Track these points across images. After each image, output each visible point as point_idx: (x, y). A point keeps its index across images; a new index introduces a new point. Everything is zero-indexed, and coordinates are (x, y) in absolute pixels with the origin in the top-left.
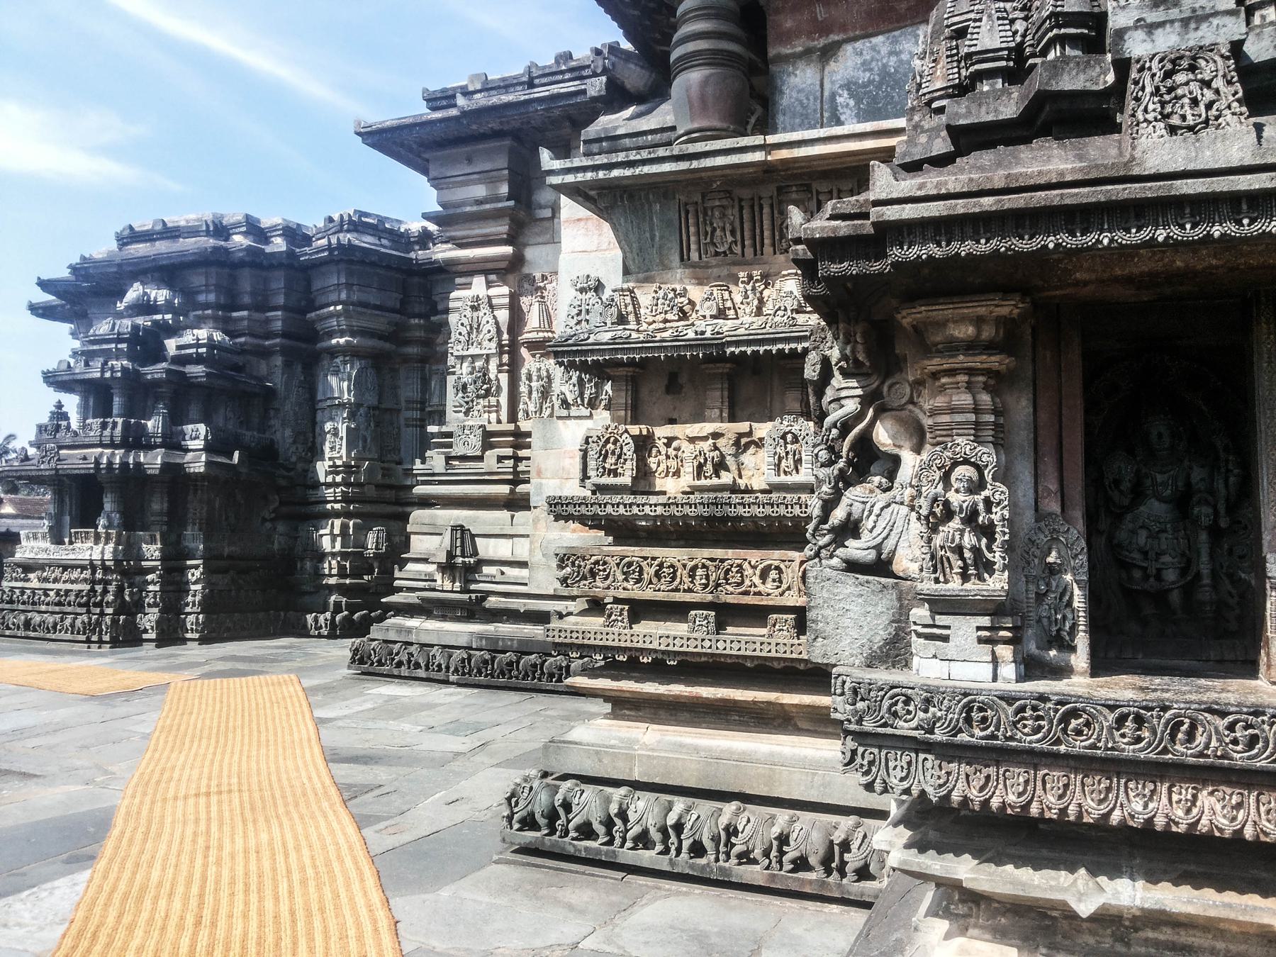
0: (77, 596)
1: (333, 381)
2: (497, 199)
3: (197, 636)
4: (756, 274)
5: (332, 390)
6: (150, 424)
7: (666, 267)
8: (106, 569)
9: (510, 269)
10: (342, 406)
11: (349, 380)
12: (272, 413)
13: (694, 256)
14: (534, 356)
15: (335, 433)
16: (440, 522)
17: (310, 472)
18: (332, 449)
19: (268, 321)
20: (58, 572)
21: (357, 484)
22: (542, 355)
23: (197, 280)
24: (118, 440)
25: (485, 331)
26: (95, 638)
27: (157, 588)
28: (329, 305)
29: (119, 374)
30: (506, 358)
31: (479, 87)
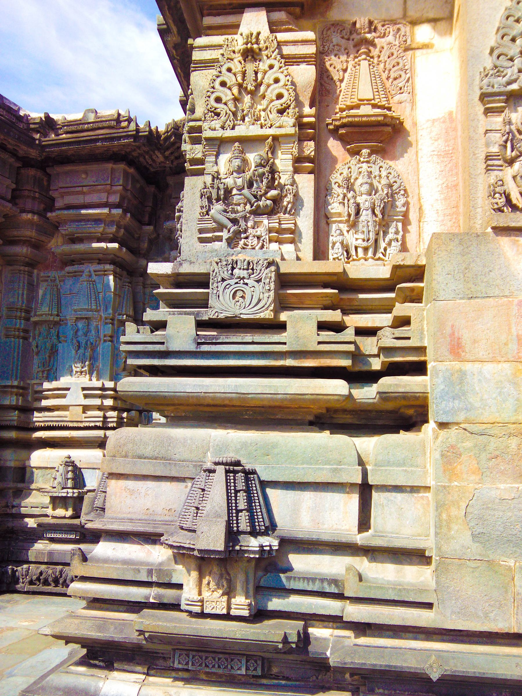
16: (181, 453)
25: (271, 93)
30: (309, 148)
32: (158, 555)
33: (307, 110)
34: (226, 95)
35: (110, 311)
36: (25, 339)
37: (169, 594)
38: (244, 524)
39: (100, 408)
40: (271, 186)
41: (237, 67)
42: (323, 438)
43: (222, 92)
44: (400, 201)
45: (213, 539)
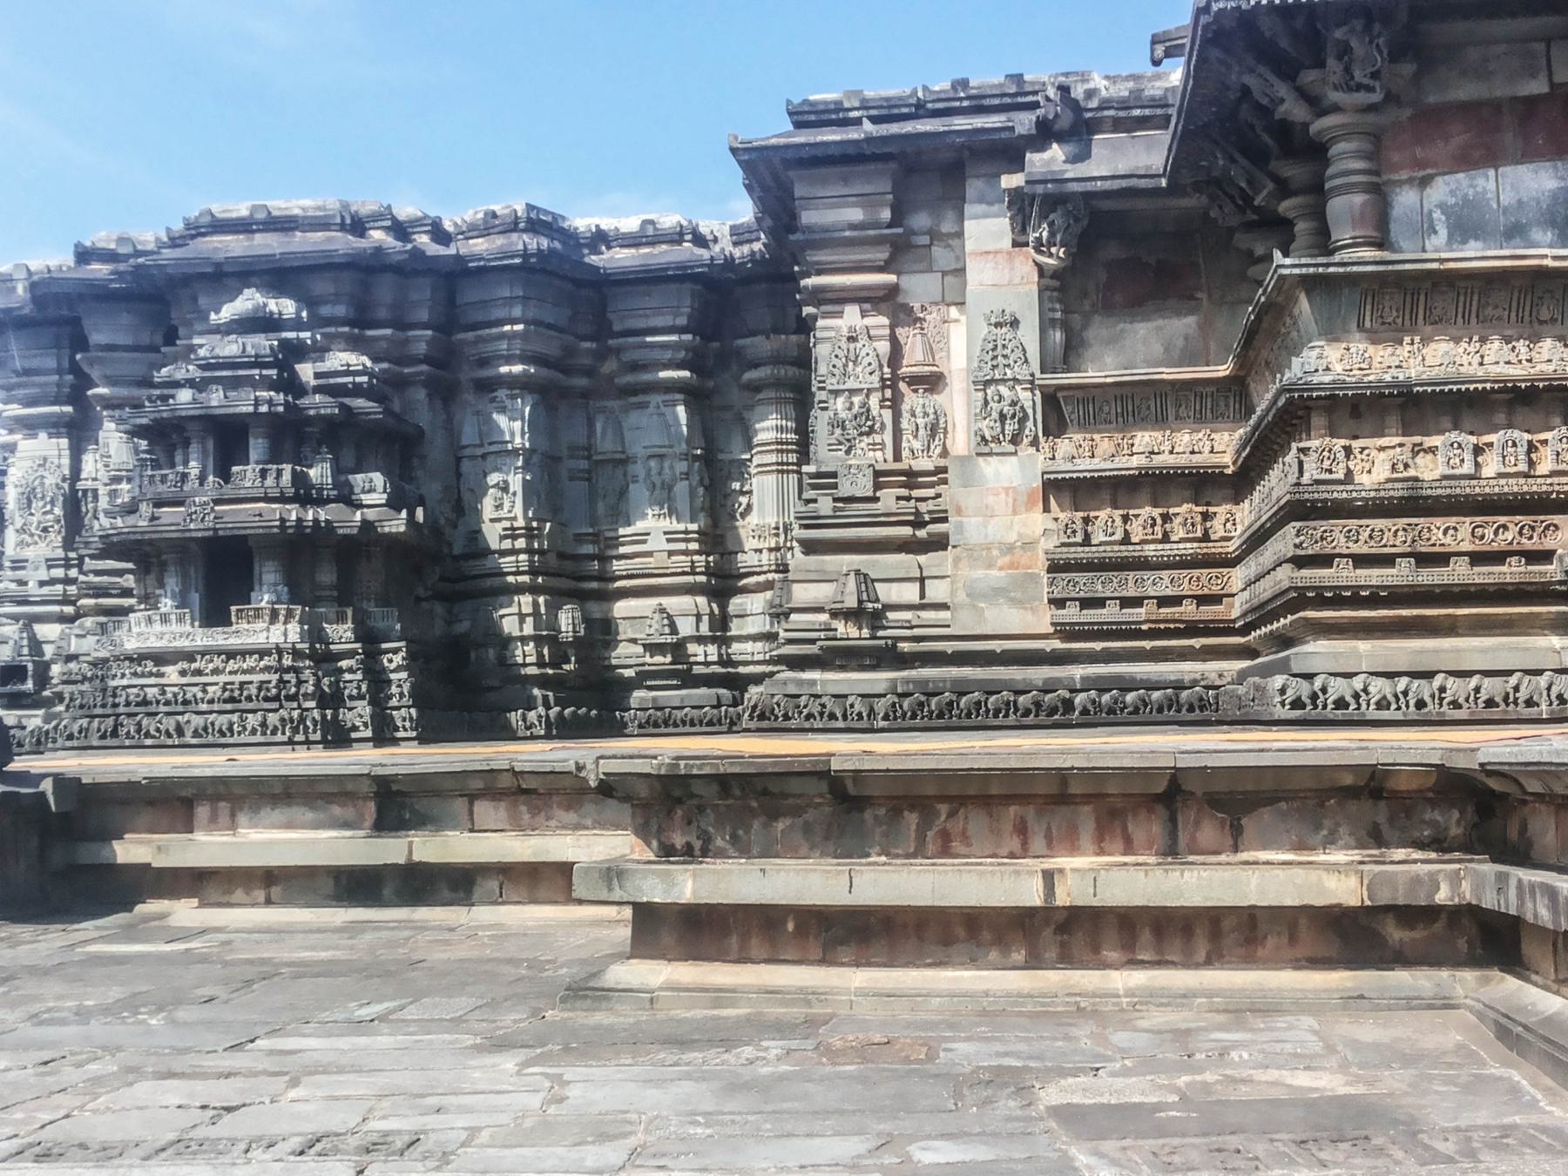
0: (260, 689)
1: (502, 420)
2: (876, 225)
3: (414, 734)
4: (1417, 339)
5: (502, 432)
6: (312, 472)
7: (1348, 332)
8: (297, 654)
9: (885, 300)
10: (515, 452)
11: (523, 419)
12: (415, 462)
13: (1368, 324)
14: (915, 391)
15: (504, 488)
16: (830, 568)
17: (476, 534)
18: (499, 507)
19: (407, 341)
20: (218, 662)
21: (541, 552)
22: (926, 390)
23: (321, 286)
24: (290, 492)
26: (300, 737)
27: (359, 676)
28: (502, 323)
29: (281, 409)
30: (888, 393)
31: (857, 104)
32: (824, 617)
33: (886, 370)
34: (839, 364)
35: (684, 446)
36: (589, 480)
37: (831, 634)
38: (865, 597)
39: (685, 553)
40: (867, 419)
41: (844, 346)
42: (902, 557)
43: (835, 361)
44: (942, 421)
45: (851, 602)
